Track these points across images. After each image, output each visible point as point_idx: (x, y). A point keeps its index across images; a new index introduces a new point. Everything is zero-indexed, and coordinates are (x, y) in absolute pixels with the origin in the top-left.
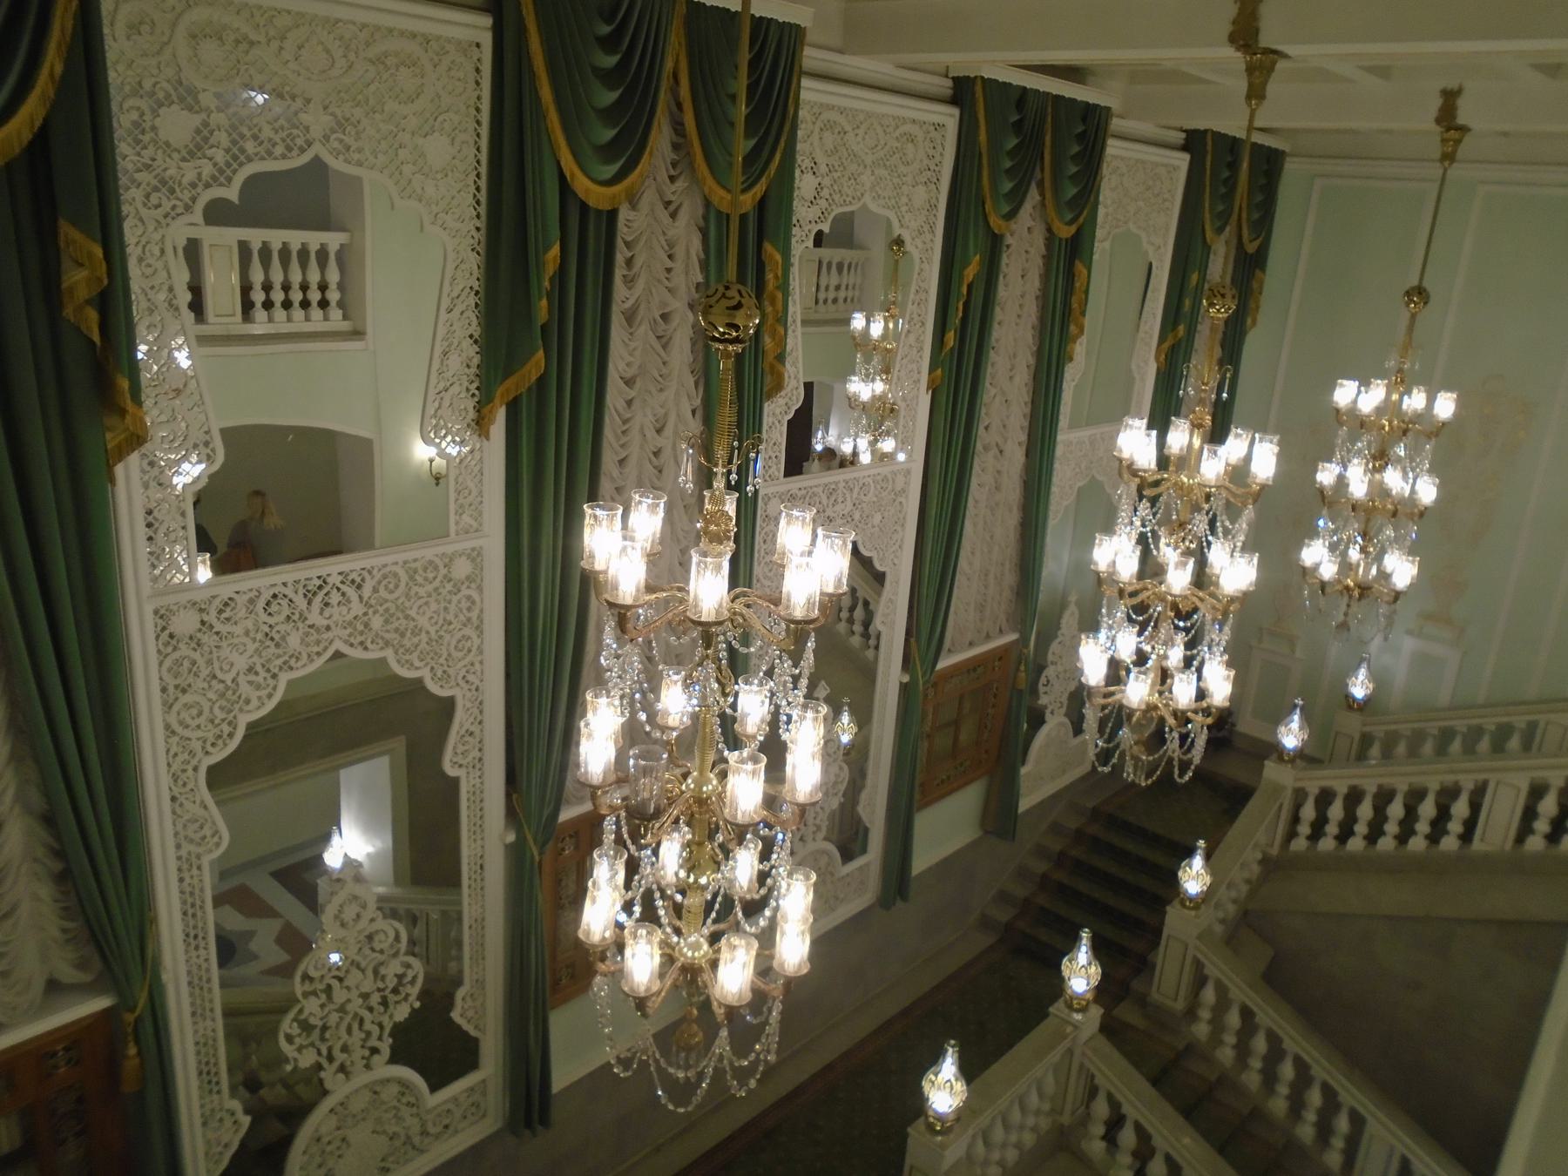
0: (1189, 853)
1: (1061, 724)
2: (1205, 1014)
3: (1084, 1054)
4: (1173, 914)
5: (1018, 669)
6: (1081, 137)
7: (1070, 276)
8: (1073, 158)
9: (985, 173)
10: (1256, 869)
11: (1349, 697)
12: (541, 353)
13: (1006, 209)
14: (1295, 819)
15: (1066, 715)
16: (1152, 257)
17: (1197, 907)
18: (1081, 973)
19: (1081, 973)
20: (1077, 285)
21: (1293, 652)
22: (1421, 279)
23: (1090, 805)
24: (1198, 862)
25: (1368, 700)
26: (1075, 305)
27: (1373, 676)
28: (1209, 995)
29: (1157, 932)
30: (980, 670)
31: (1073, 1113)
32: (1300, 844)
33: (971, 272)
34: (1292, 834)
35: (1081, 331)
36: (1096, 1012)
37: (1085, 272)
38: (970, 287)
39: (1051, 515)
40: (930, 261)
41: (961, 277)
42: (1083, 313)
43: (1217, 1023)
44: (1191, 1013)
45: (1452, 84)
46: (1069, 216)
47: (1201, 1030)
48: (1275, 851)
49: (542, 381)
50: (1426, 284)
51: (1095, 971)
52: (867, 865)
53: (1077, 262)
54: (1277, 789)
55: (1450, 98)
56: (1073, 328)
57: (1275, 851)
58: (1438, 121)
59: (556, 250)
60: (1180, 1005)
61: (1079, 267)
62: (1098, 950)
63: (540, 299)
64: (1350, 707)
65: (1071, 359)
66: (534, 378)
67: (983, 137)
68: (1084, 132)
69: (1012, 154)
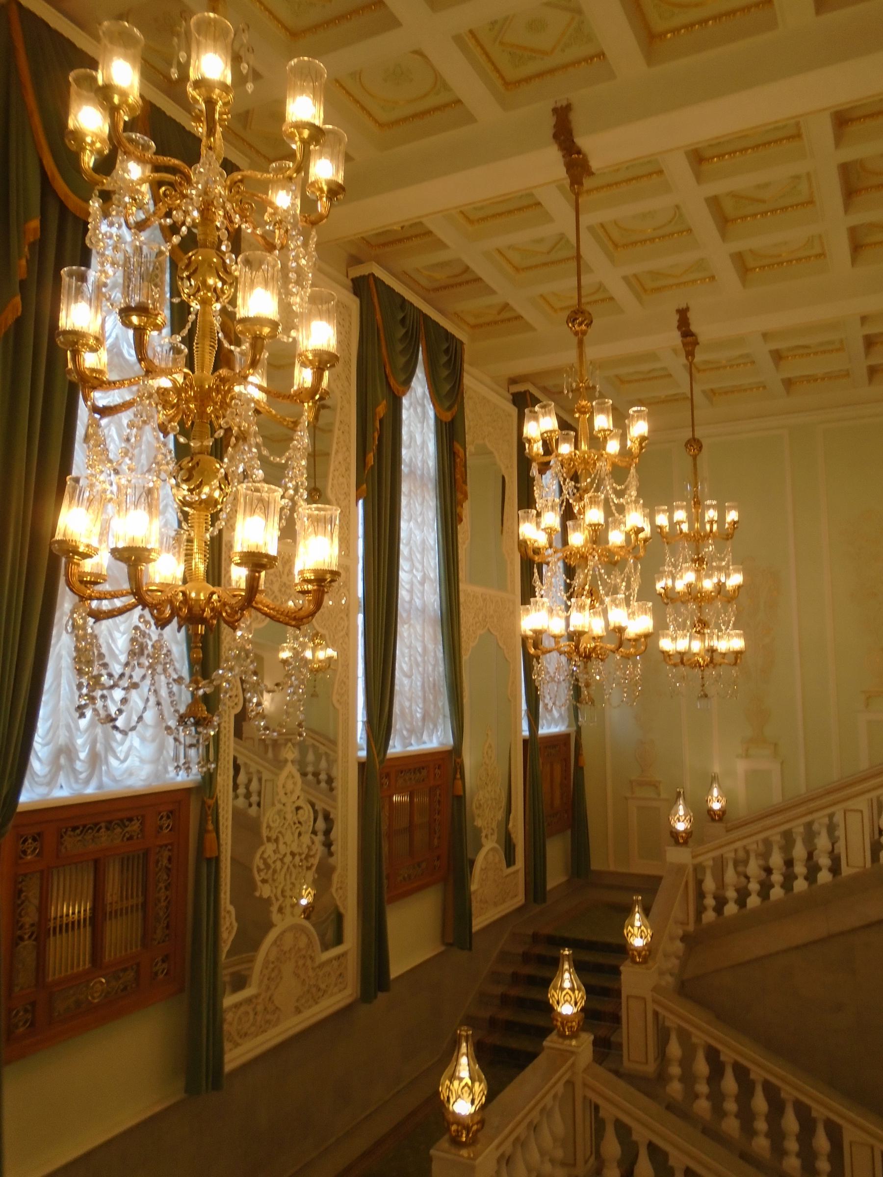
0: (628, 912)
1: (493, 849)
2: (675, 1070)
3: (585, 1085)
4: (627, 970)
5: (455, 778)
6: (447, 351)
7: (453, 454)
8: (444, 365)
9: (383, 343)
10: (679, 946)
11: (710, 811)
12: (18, 299)
13: (403, 377)
14: (701, 895)
15: (497, 842)
16: (504, 472)
17: (645, 960)
18: (567, 999)
19: (567, 999)
20: (458, 460)
21: (659, 795)
22: (693, 435)
23: (530, 932)
24: (637, 919)
25: (723, 811)
26: (458, 476)
27: (724, 792)
28: (674, 1049)
29: (618, 993)
30: (424, 772)
31: (586, 1162)
32: (709, 916)
33: (382, 410)
34: (700, 910)
35: (466, 497)
36: (587, 1039)
37: (461, 450)
38: (381, 421)
39: (463, 652)
40: (349, 402)
41: (374, 415)
42: (465, 482)
43: (688, 1078)
44: (662, 1077)
45: (683, 306)
46: (447, 404)
47: (675, 1088)
48: (691, 928)
49: (19, 323)
50: (696, 436)
51: (579, 995)
52: (344, 954)
53: (455, 443)
54: (680, 869)
55: (683, 315)
56: (460, 496)
57: (691, 928)
58: (679, 328)
59: (35, 223)
60: (651, 1068)
61: (458, 447)
62: (580, 968)
63: (20, 258)
64: (713, 820)
65: (461, 520)
66: (11, 320)
67: (379, 317)
68: (448, 348)
69: (402, 340)
